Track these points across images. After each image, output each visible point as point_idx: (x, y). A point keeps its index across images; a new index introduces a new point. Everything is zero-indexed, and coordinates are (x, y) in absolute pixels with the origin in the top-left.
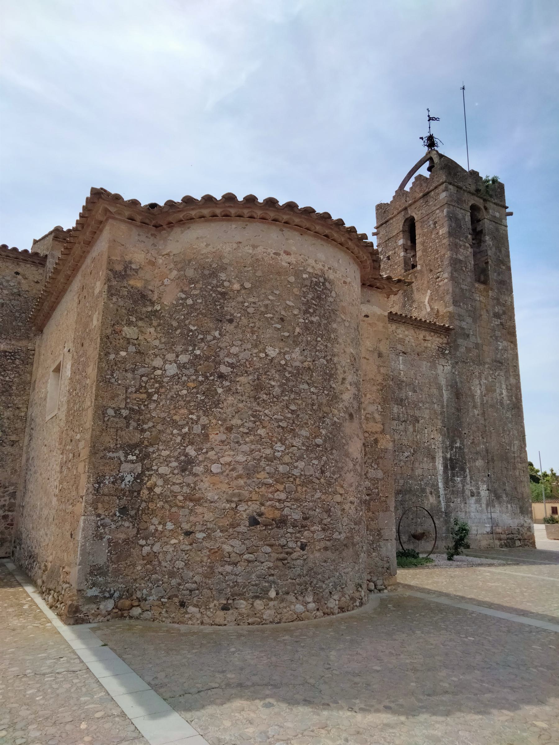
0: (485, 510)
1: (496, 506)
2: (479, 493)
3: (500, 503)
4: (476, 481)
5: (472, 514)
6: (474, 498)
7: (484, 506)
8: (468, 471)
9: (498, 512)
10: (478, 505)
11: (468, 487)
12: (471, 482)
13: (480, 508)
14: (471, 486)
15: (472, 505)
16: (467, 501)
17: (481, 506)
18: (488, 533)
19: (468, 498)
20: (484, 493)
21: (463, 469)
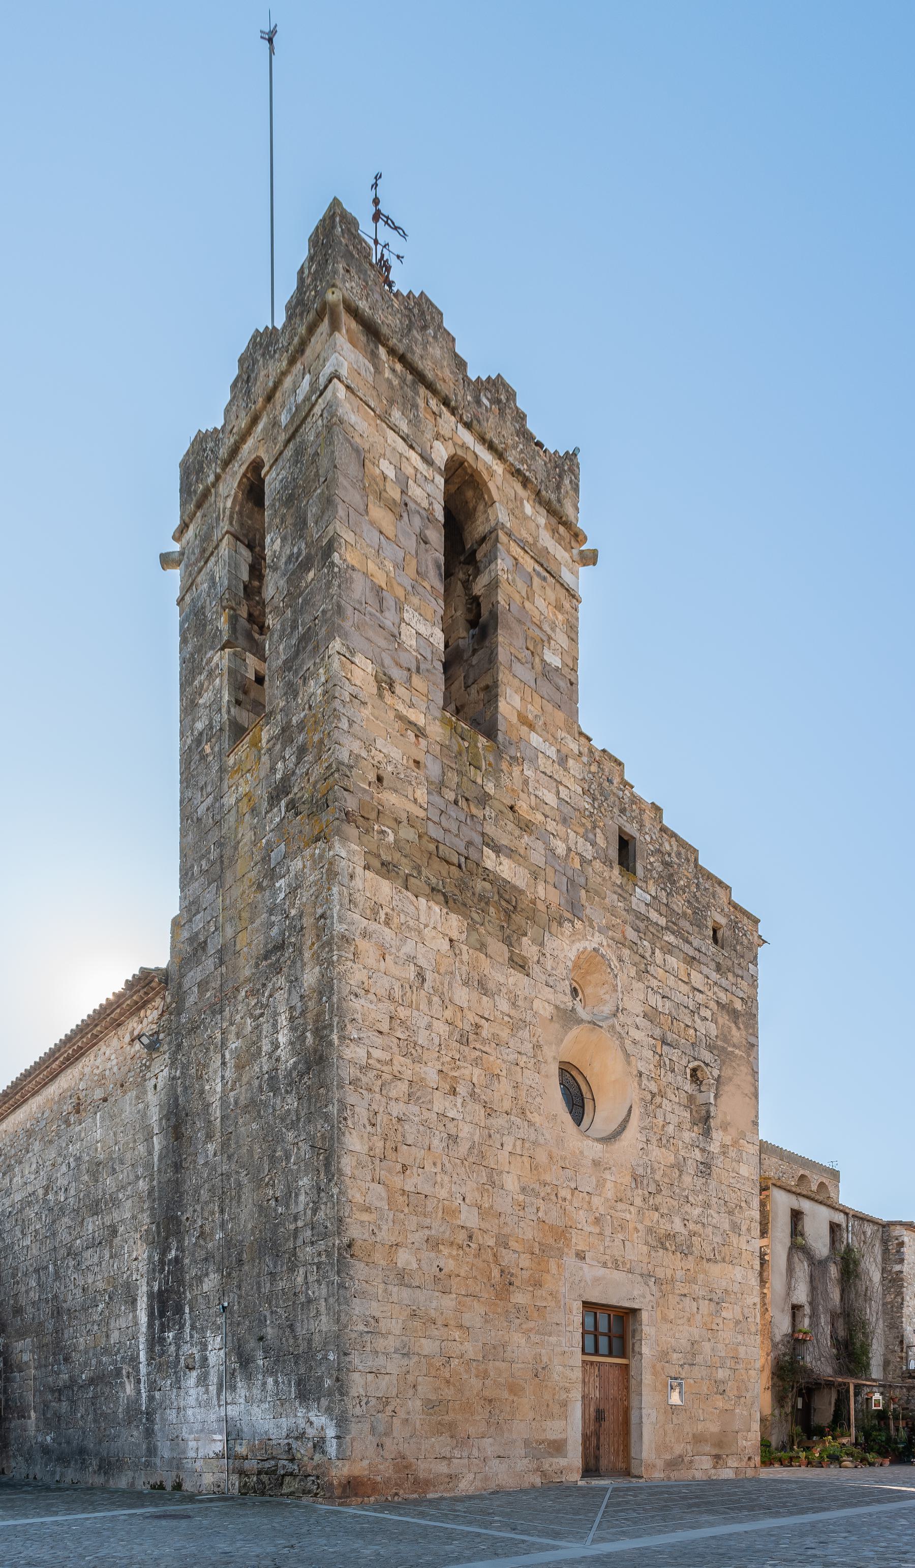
0: (215, 1398)
1: (239, 1385)
2: (205, 1359)
3: (249, 1377)
4: (203, 1330)
5: (190, 1412)
6: (194, 1374)
7: (213, 1389)
8: (187, 1310)
9: (242, 1401)
10: (201, 1389)
11: (186, 1349)
12: (192, 1337)
13: (205, 1397)
14: (192, 1345)
15: (192, 1392)
16: (182, 1383)
17: (207, 1392)
18: (218, 1456)
19: (185, 1374)
20: (216, 1357)
21: (179, 1310)
